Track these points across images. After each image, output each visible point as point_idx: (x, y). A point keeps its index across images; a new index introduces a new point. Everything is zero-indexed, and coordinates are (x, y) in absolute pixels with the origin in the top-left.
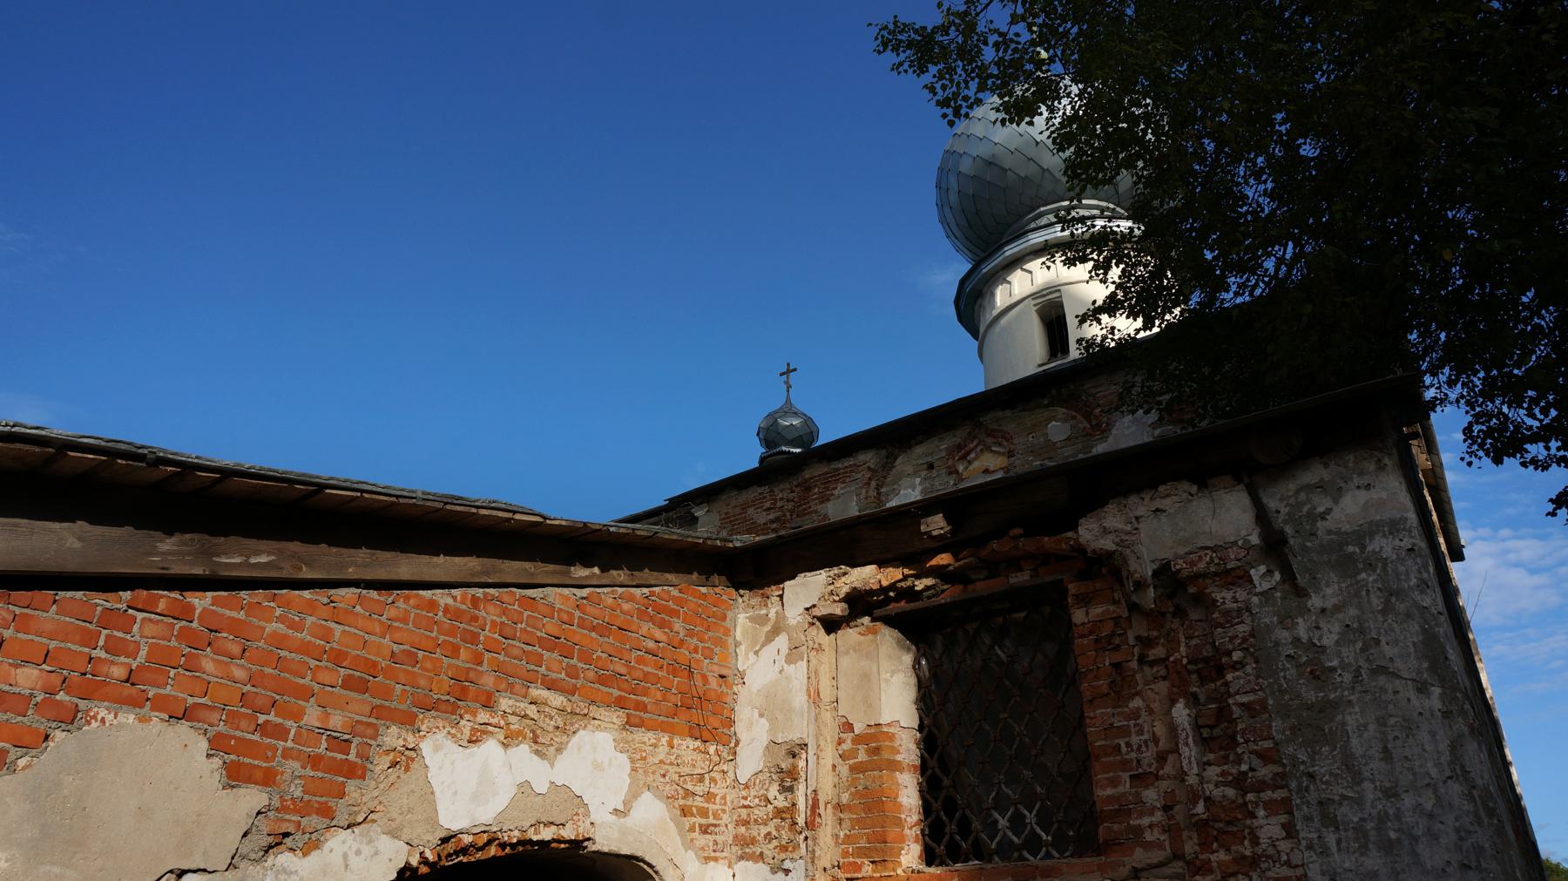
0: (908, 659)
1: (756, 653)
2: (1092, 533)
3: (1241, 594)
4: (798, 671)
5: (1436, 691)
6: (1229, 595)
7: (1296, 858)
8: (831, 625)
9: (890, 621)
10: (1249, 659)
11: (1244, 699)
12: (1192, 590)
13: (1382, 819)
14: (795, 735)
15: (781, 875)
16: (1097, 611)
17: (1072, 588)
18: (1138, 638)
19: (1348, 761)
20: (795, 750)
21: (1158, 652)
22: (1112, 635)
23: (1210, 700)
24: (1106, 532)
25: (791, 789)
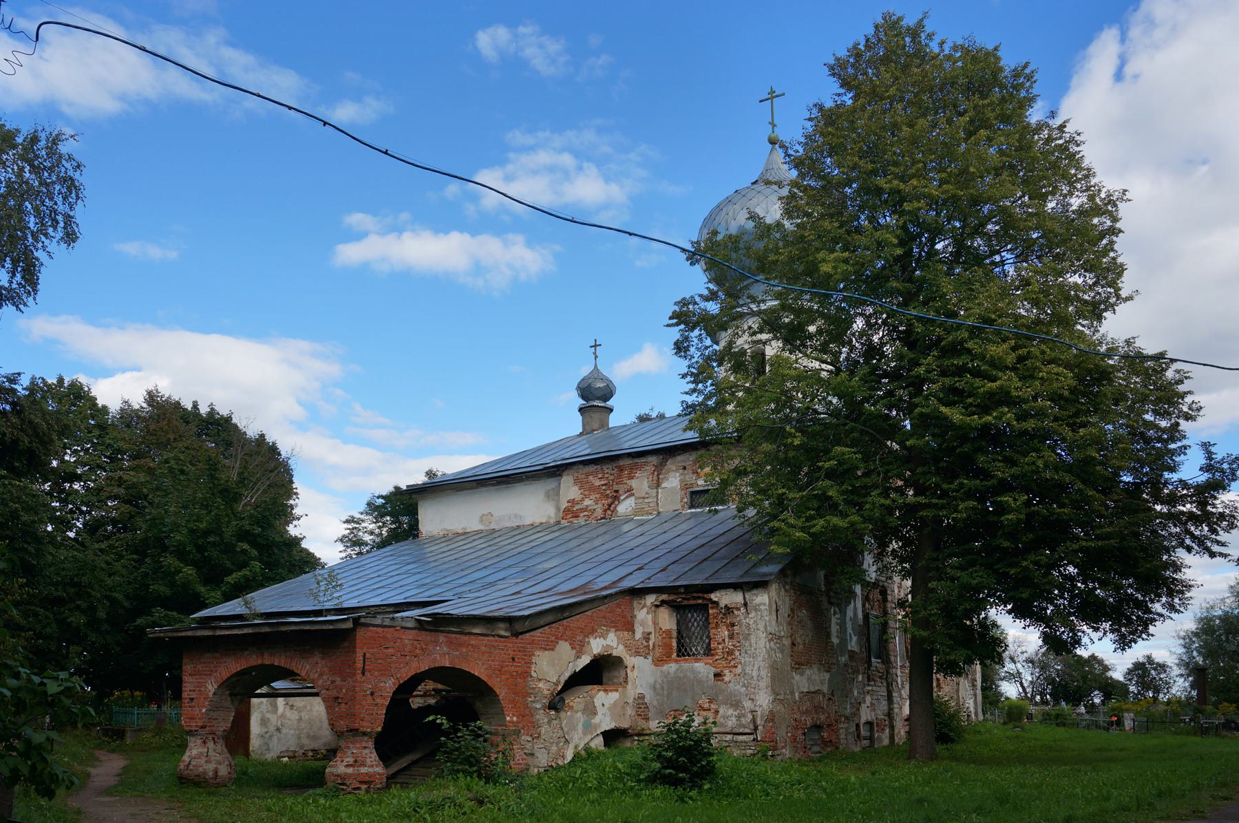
2: (714, 596)
8: (657, 606)
20: (649, 634)
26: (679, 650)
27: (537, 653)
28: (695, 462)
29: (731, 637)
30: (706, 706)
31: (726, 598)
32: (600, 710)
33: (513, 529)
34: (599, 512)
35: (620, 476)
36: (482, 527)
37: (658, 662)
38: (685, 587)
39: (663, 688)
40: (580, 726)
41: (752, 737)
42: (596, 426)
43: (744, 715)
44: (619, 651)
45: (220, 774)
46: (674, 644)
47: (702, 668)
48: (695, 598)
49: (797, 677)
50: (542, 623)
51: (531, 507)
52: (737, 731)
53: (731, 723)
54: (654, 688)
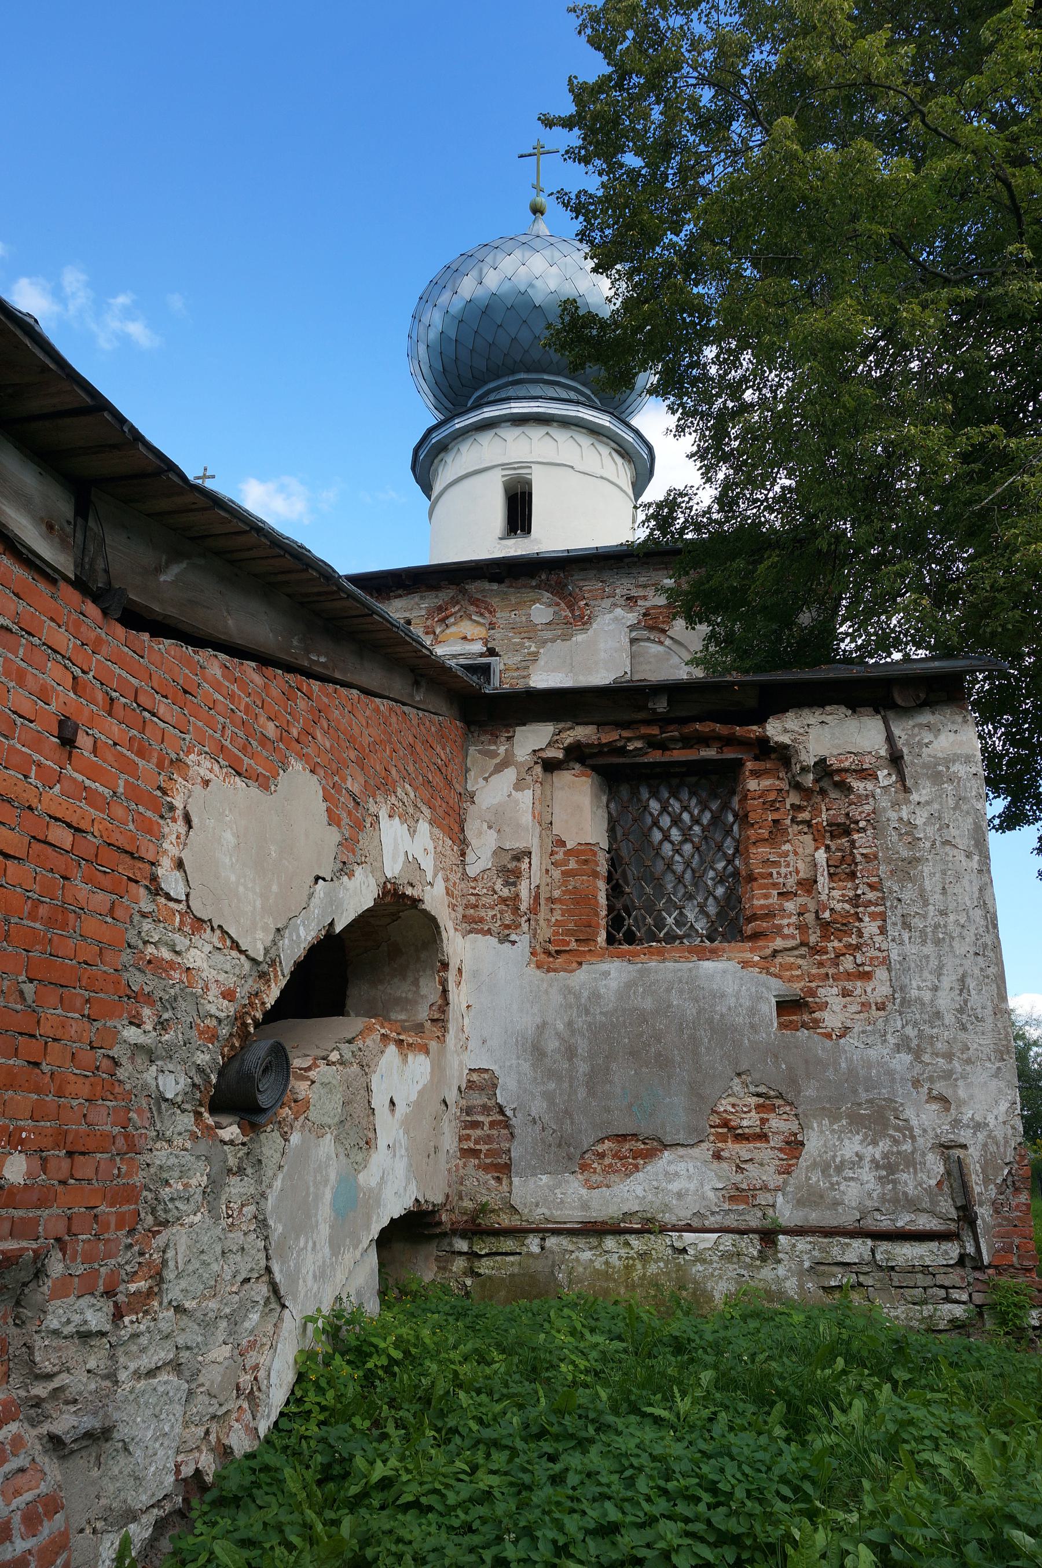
0: (604, 799)
1: (486, 779)
2: (777, 730)
3: (870, 786)
4: (526, 798)
5: (976, 858)
6: (861, 785)
7: (884, 947)
8: (550, 766)
9: (595, 769)
10: (869, 827)
11: (865, 851)
12: (837, 778)
13: (937, 926)
14: (520, 845)
15: (507, 945)
16: (766, 783)
17: (749, 765)
18: (792, 805)
19: (922, 895)
21: (805, 815)
22: (774, 801)
23: (838, 850)
24: (786, 731)
25: (514, 884)
26: (615, 922)
28: (430, 615)
29: (844, 869)
30: (750, 1121)
32: (388, 1129)
37: (551, 955)
39: (570, 1052)
40: (324, 1212)
41: (952, 1251)
43: (910, 1162)
46: (602, 900)
52: (885, 1223)
53: (858, 1192)
54: (537, 1052)
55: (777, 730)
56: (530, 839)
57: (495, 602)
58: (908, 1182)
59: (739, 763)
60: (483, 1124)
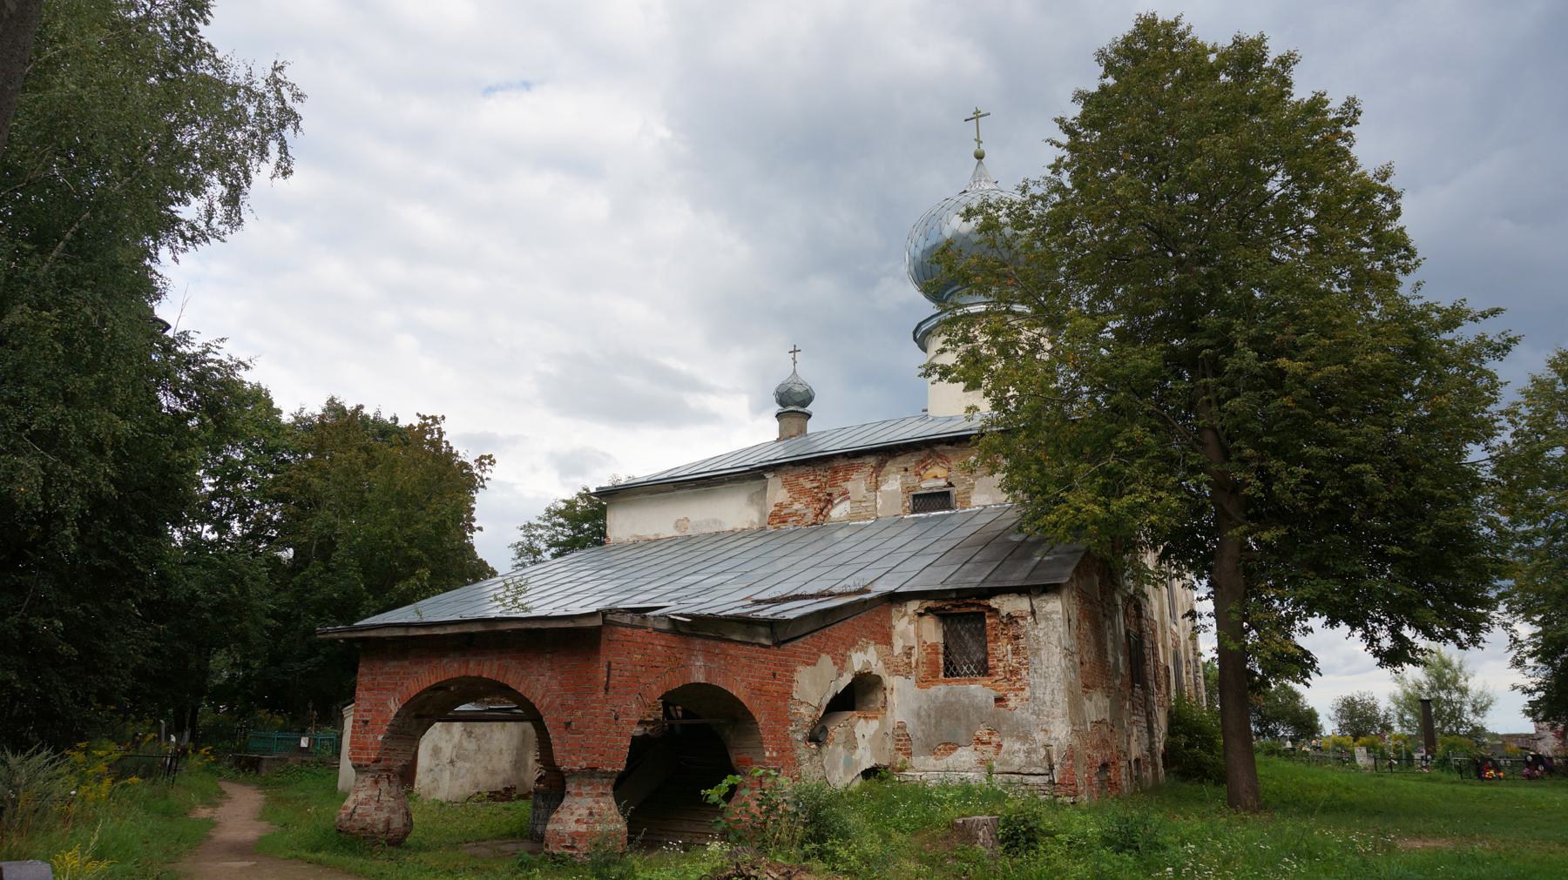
2: (993, 603)
4: (912, 627)
8: (920, 615)
20: (911, 648)
26: (947, 669)
27: (799, 668)
28: (917, 464)
29: (1016, 652)
30: (985, 738)
31: (1008, 605)
32: (861, 744)
33: (711, 535)
34: (810, 517)
35: (833, 478)
36: (676, 533)
37: (923, 683)
38: (958, 591)
40: (841, 765)
42: (794, 432)
43: (1035, 751)
44: (877, 668)
45: (393, 826)
46: (941, 662)
47: (978, 691)
48: (968, 605)
49: (1087, 702)
50: (805, 630)
51: (734, 512)
53: (1018, 761)
54: (919, 716)
55: (993, 603)
56: (914, 643)
57: (950, 456)
58: (1034, 757)
59: (983, 614)
60: (903, 740)
